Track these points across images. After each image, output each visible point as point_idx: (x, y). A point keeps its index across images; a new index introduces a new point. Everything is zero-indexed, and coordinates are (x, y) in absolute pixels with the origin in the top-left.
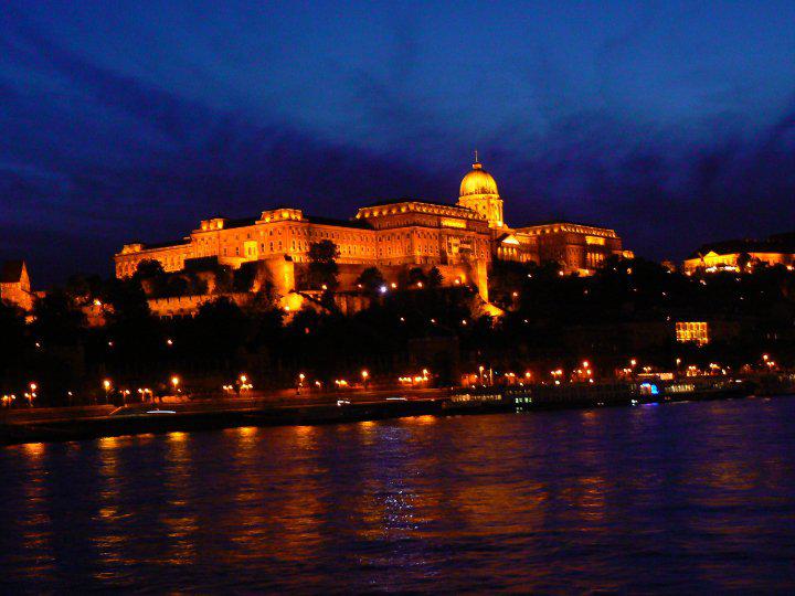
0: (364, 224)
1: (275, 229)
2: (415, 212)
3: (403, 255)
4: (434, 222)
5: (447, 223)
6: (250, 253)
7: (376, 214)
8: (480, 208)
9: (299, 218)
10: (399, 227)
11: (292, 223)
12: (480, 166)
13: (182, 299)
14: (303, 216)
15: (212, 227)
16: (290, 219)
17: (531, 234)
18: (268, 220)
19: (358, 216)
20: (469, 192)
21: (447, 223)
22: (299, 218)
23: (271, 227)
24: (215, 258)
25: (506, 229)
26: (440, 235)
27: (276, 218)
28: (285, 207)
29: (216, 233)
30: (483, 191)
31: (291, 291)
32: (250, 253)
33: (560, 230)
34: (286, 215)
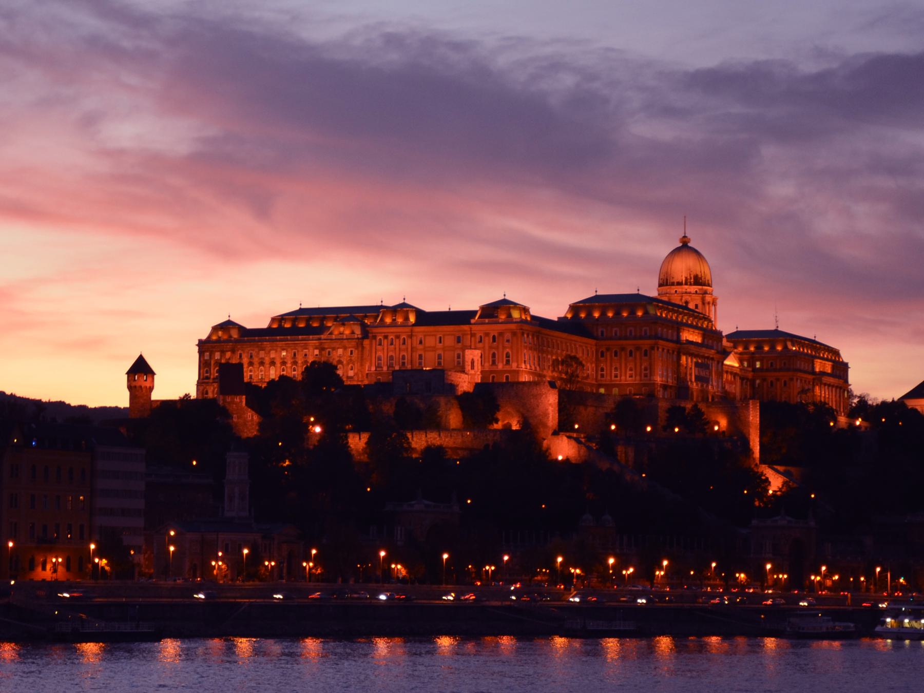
1: (501, 334)
3: (636, 380)
6: (473, 368)
10: (635, 338)
24: (200, 341)
29: (408, 329)
32: (473, 368)
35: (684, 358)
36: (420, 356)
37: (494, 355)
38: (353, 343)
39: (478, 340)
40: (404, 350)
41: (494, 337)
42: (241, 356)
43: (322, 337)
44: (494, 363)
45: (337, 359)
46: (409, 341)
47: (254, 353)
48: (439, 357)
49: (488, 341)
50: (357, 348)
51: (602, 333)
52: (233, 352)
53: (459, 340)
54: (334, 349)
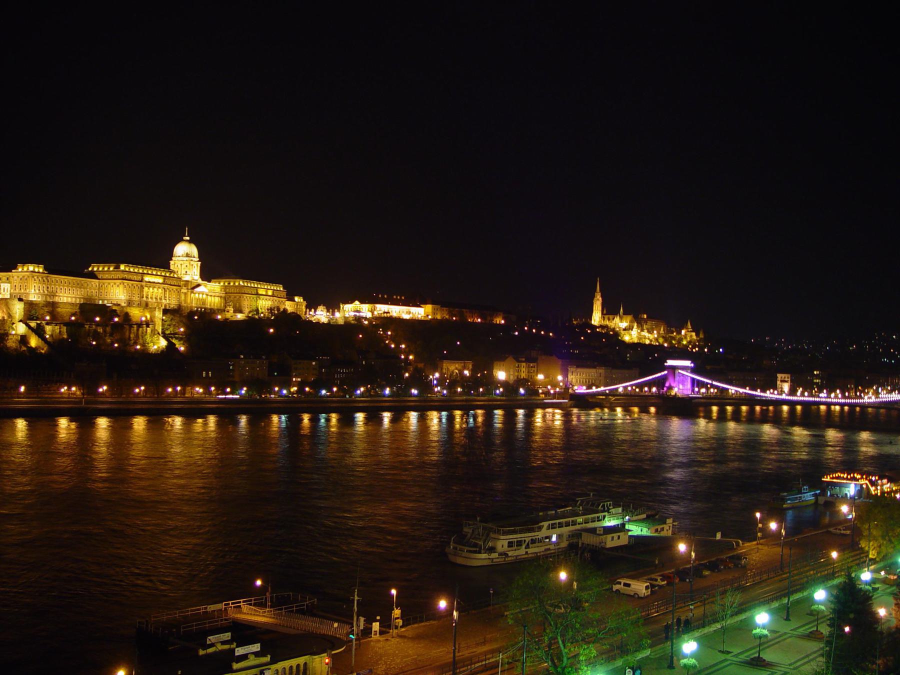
0: (93, 276)
4: (140, 278)
5: (147, 278)
8: (184, 266)
9: (41, 270)
12: (188, 238)
14: (45, 269)
17: (222, 284)
18: (20, 270)
19: (90, 269)
21: (147, 278)
22: (41, 270)
25: (200, 281)
27: (25, 269)
28: (31, 263)
30: (187, 255)
31: (21, 321)
34: (31, 268)
35: (146, 289)
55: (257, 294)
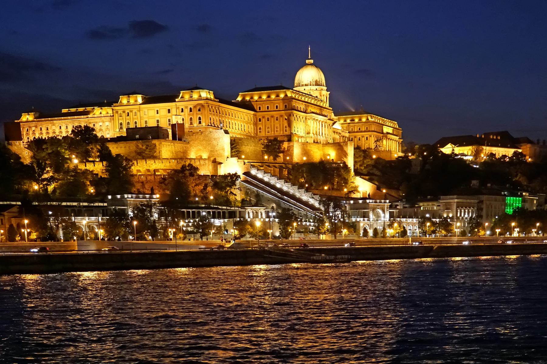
1: (195, 107)
2: (292, 98)
7: (256, 98)
9: (212, 97)
11: (210, 102)
13: (149, 162)
14: (215, 97)
15: (132, 101)
16: (207, 99)
18: (187, 97)
19: (239, 99)
20: (304, 84)
23: (191, 105)
26: (306, 118)
30: (317, 84)
33: (368, 119)
34: (204, 94)
36: (146, 122)
37: (191, 119)
38: (108, 118)
39: (181, 110)
40: (135, 119)
41: (191, 108)
42: (41, 128)
43: (89, 116)
44: (191, 124)
45: (99, 128)
46: (138, 114)
47: (49, 127)
48: (158, 121)
49: (187, 111)
50: (110, 122)
51: (260, 108)
52: (36, 127)
53: (169, 111)
54: (96, 123)
55: (383, 133)
